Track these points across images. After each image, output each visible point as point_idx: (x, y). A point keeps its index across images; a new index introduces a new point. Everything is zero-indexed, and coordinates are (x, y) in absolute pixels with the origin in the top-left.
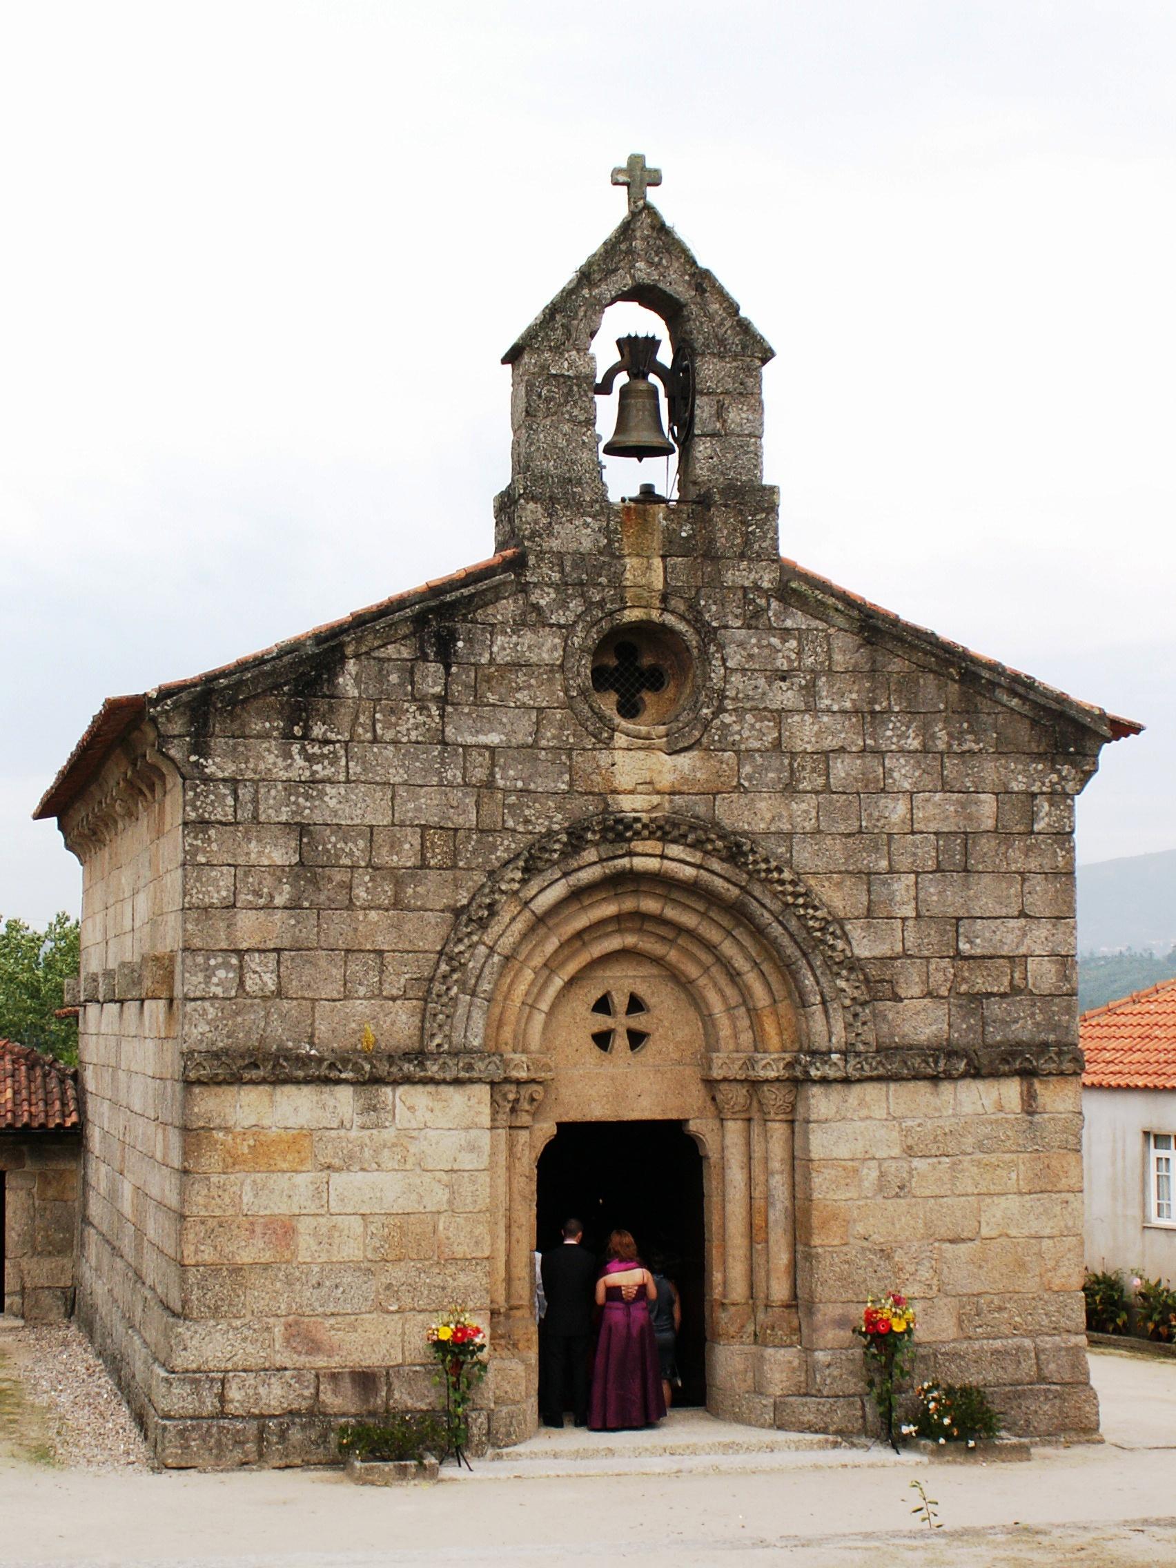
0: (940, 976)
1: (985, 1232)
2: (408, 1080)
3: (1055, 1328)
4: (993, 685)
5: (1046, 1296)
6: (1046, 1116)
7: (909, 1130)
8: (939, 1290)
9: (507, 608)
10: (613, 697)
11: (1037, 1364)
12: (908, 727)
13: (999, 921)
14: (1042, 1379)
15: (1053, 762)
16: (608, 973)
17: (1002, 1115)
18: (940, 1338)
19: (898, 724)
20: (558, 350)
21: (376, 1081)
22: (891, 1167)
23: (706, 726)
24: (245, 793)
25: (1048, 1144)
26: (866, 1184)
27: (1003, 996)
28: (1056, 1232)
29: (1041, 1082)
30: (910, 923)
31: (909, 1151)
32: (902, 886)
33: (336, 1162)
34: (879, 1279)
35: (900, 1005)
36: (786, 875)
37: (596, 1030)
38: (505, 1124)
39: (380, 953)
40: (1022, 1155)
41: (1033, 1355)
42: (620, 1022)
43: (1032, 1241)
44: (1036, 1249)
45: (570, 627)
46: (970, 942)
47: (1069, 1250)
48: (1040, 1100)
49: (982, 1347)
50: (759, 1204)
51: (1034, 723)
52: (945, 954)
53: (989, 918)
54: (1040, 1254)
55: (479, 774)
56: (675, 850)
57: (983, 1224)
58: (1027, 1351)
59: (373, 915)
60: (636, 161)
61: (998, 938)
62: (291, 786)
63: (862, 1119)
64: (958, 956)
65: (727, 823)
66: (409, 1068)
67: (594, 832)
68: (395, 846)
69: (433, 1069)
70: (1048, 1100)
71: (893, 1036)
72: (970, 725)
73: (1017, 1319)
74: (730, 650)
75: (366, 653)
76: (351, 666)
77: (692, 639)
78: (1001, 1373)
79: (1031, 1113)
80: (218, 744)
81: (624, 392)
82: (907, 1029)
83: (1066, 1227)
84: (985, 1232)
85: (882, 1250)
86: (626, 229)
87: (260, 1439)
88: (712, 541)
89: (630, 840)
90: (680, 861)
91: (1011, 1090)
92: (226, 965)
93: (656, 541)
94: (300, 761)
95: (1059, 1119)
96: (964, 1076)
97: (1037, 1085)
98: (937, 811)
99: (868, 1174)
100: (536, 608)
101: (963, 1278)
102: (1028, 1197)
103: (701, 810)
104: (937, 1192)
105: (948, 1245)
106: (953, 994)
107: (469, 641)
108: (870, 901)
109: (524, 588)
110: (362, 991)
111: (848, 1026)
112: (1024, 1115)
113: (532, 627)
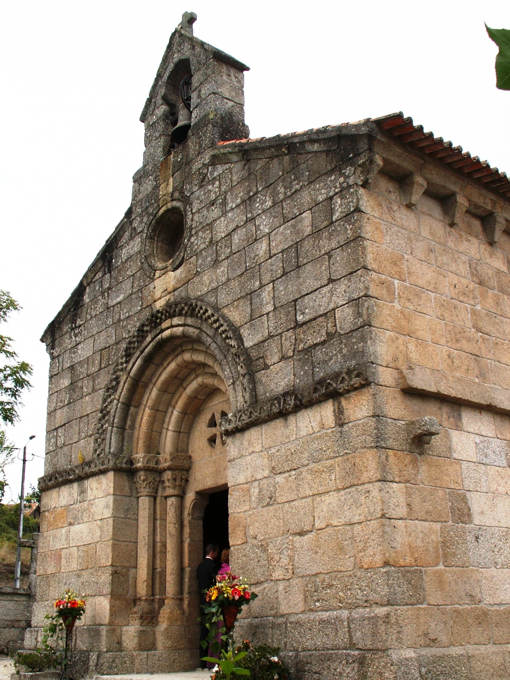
0: (288, 343)
1: (318, 525)
3: (366, 601)
4: (302, 143)
5: (359, 573)
6: (350, 425)
7: (272, 455)
8: (293, 573)
11: (349, 631)
12: (266, 196)
13: (317, 292)
14: (352, 646)
15: (340, 170)
16: (213, 403)
17: (325, 431)
18: (294, 611)
19: (261, 197)
25: (354, 446)
26: (253, 499)
27: (323, 343)
28: (362, 518)
29: (346, 399)
30: (271, 315)
31: (274, 471)
32: (266, 294)
34: (261, 567)
35: (269, 371)
37: (209, 436)
38: (145, 493)
40: (337, 460)
41: (346, 623)
43: (348, 528)
44: (350, 534)
46: (303, 313)
47: (373, 532)
48: (346, 413)
49: (315, 618)
51: (327, 152)
52: (289, 327)
53: (312, 292)
54: (352, 538)
57: (316, 518)
58: (342, 621)
61: (317, 304)
63: (250, 454)
64: (298, 325)
67: (147, 326)
70: (351, 412)
71: (265, 393)
72: (295, 176)
73: (341, 594)
75: (91, 281)
78: (325, 639)
79: (342, 425)
82: (273, 386)
83: (369, 512)
84: (318, 525)
85: (262, 545)
89: (160, 324)
91: (327, 411)
95: (359, 425)
97: (344, 402)
98: (282, 238)
99: (254, 492)
101: (308, 563)
102: (343, 492)
104: (290, 498)
105: (298, 537)
106: (296, 353)
108: (252, 310)
112: (337, 427)
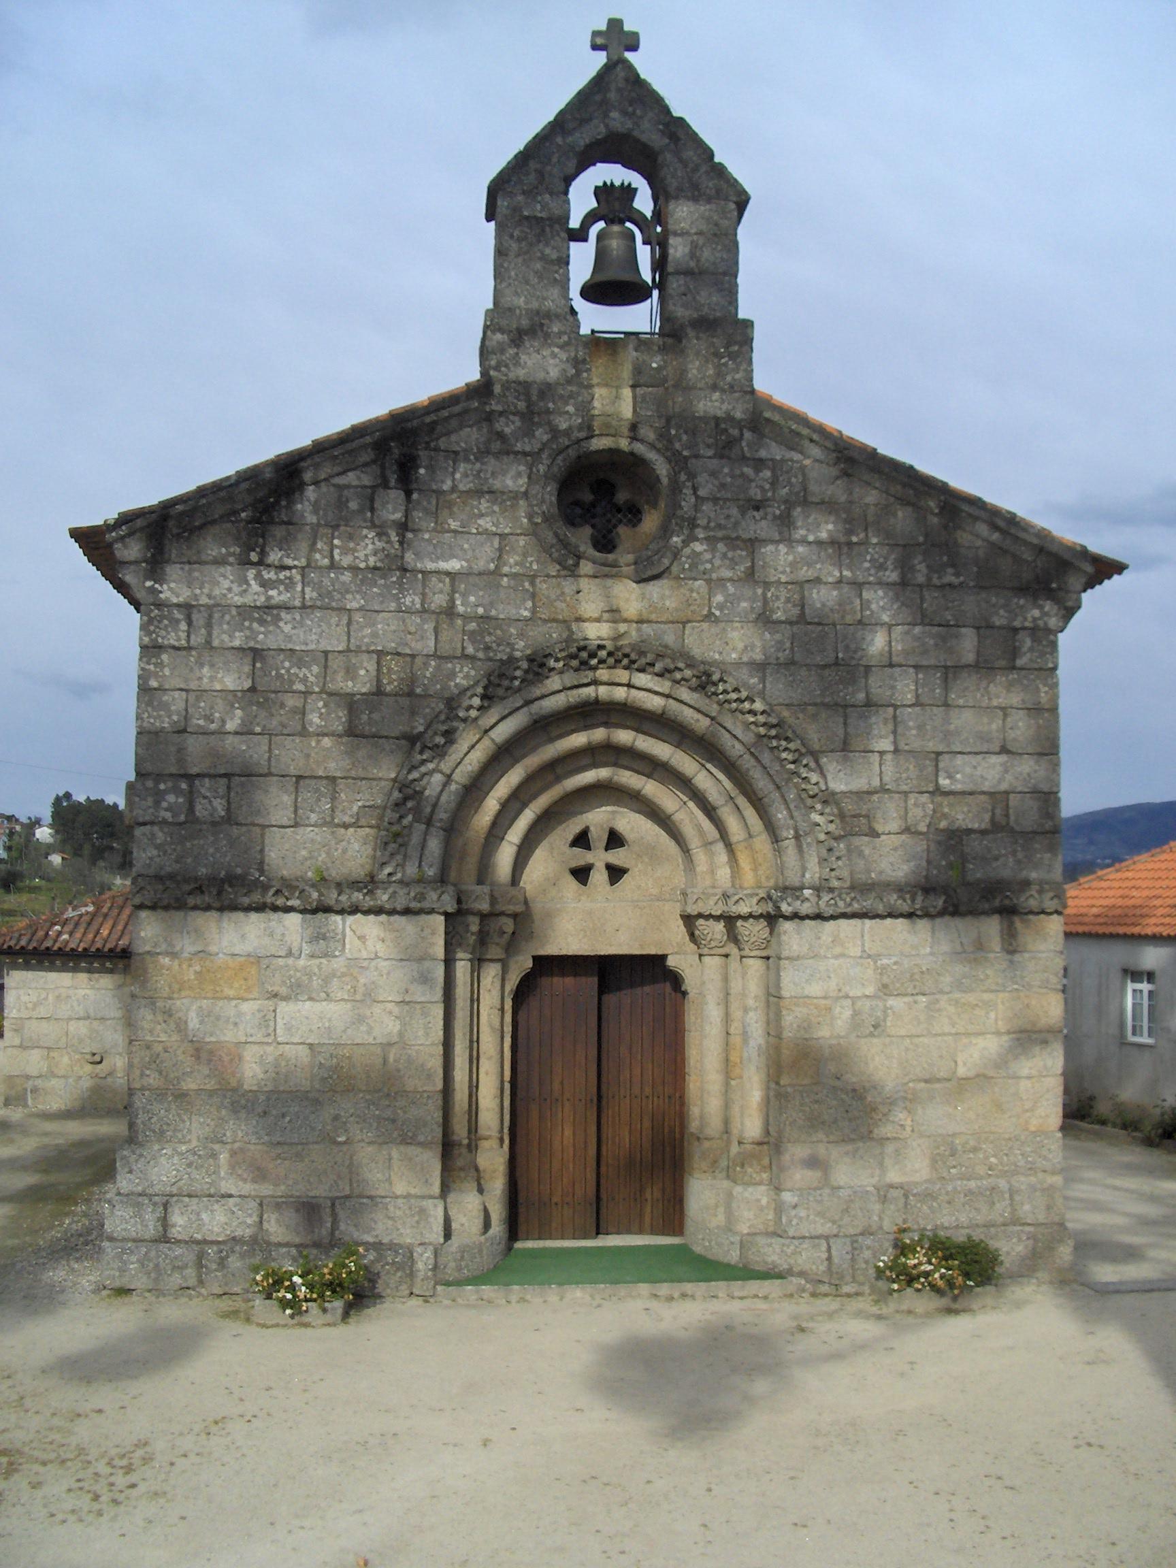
2: (355, 910)
7: (884, 968)
8: (913, 1131)
9: (469, 437)
10: (587, 531)
11: (1011, 1205)
20: (531, 193)
21: (327, 910)
22: (865, 1005)
23: (676, 555)
24: (199, 619)
29: (1023, 921)
30: (889, 757)
31: (885, 990)
33: (284, 991)
34: (850, 1120)
36: (758, 706)
39: (332, 780)
41: (1007, 1196)
42: (599, 858)
45: (535, 455)
46: (950, 777)
47: (1048, 1091)
49: (955, 1188)
50: (736, 1040)
52: (924, 789)
53: (970, 753)
55: (439, 601)
56: (642, 679)
57: (960, 1063)
59: (327, 742)
60: (615, 25)
62: (245, 611)
63: (836, 957)
64: (938, 791)
65: (697, 652)
66: (358, 896)
68: (350, 672)
69: (383, 897)
71: (869, 871)
73: (992, 1160)
74: (702, 478)
75: (325, 480)
76: (311, 492)
77: (662, 469)
80: (174, 571)
81: (601, 236)
86: (599, 82)
87: (199, 1265)
88: (684, 372)
89: (595, 668)
90: (647, 691)
92: (177, 791)
93: (626, 372)
94: (255, 587)
96: (941, 914)
97: (1018, 924)
100: (501, 436)
103: (670, 639)
107: (431, 468)
108: (846, 734)
109: (489, 418)
110: (314, 817)
111: (823, 861)
113: (497, 455)
